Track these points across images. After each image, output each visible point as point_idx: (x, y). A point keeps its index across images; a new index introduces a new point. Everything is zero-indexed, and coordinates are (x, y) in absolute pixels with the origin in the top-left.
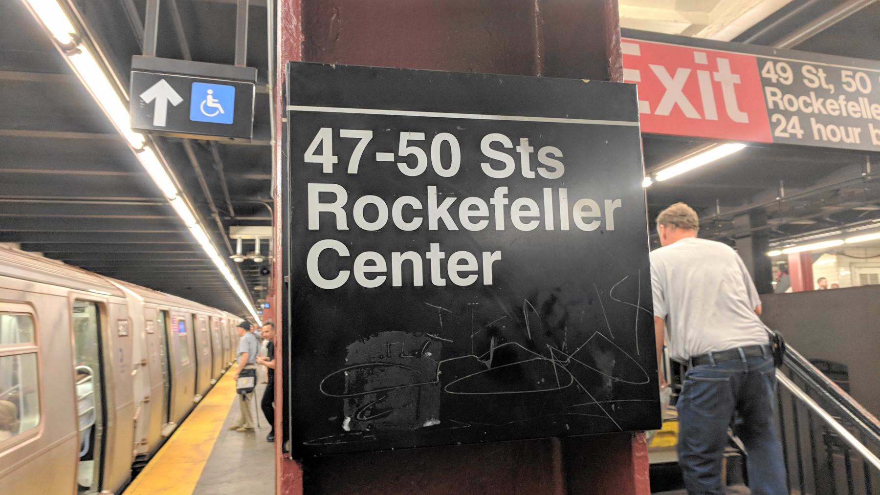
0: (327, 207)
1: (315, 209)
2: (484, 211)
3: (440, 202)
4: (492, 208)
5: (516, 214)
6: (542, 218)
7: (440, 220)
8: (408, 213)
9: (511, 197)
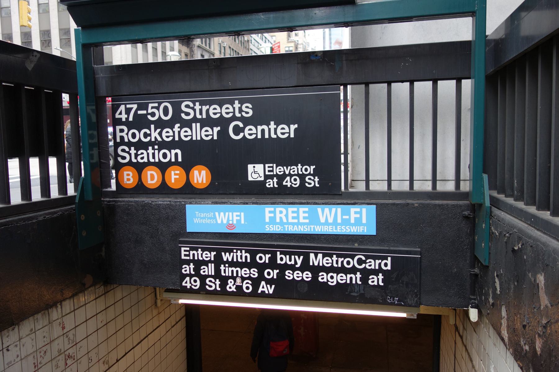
2: (171, 133)
3: (155, 131)
4: (174, 132)
6: (192, 136)
7: (155, 138)
8: (146, 135)
9: (181, 128)
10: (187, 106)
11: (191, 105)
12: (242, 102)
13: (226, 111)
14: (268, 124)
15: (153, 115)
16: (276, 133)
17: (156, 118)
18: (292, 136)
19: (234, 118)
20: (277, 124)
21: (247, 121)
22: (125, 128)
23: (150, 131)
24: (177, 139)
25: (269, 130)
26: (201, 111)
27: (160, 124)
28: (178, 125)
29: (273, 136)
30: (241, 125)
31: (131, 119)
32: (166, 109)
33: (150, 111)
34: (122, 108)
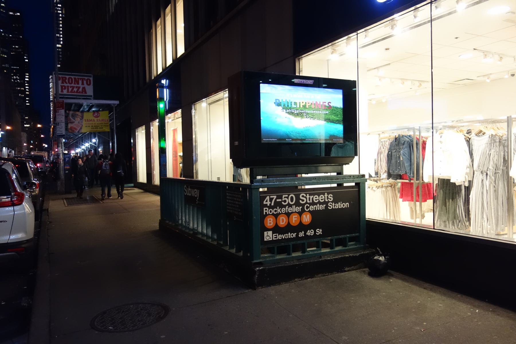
0: (266, 211)
1: (265, 211)
2: (285, 210)
3: (279, 209)
4: (286, 209)
5: (289, 210)
7: (279, 212)
8: (275, 211)
9: (288, 207)
16: (319, 208)
22: (267, 209)
23: (277, 209)
24: (287, 212)
25: (317, 207)
28: (287, 206)
29: (318, 209)
30: (309, 206)
31: (272, 204)
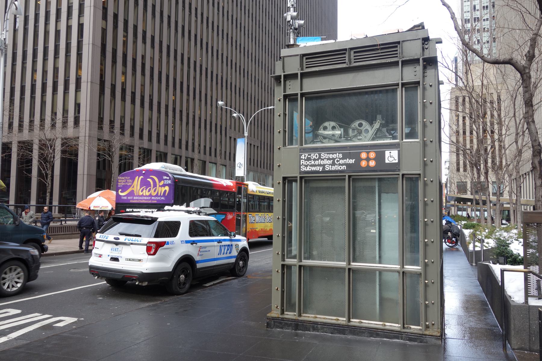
1: (302, 162)
8: (310, 163)
9: (321, 160)
10: (323, 155)
11: (324, 154)
12: (339, 153)
13: (334, 156)
14: (347, 159)
15: (313, 157)
17: (313, 158)
18: (353, 162)
19: (337, 158)
20: (349, 159)
21: (340, 159)
22: (304, 161)
24: (319, 164)
26: (327, 156)
27: (315, 160)
29: (348, 163)
30: (339, 160)
31: (306, 158)
32: (316, 156)
33: (312, 156)
34: (303, 155)
